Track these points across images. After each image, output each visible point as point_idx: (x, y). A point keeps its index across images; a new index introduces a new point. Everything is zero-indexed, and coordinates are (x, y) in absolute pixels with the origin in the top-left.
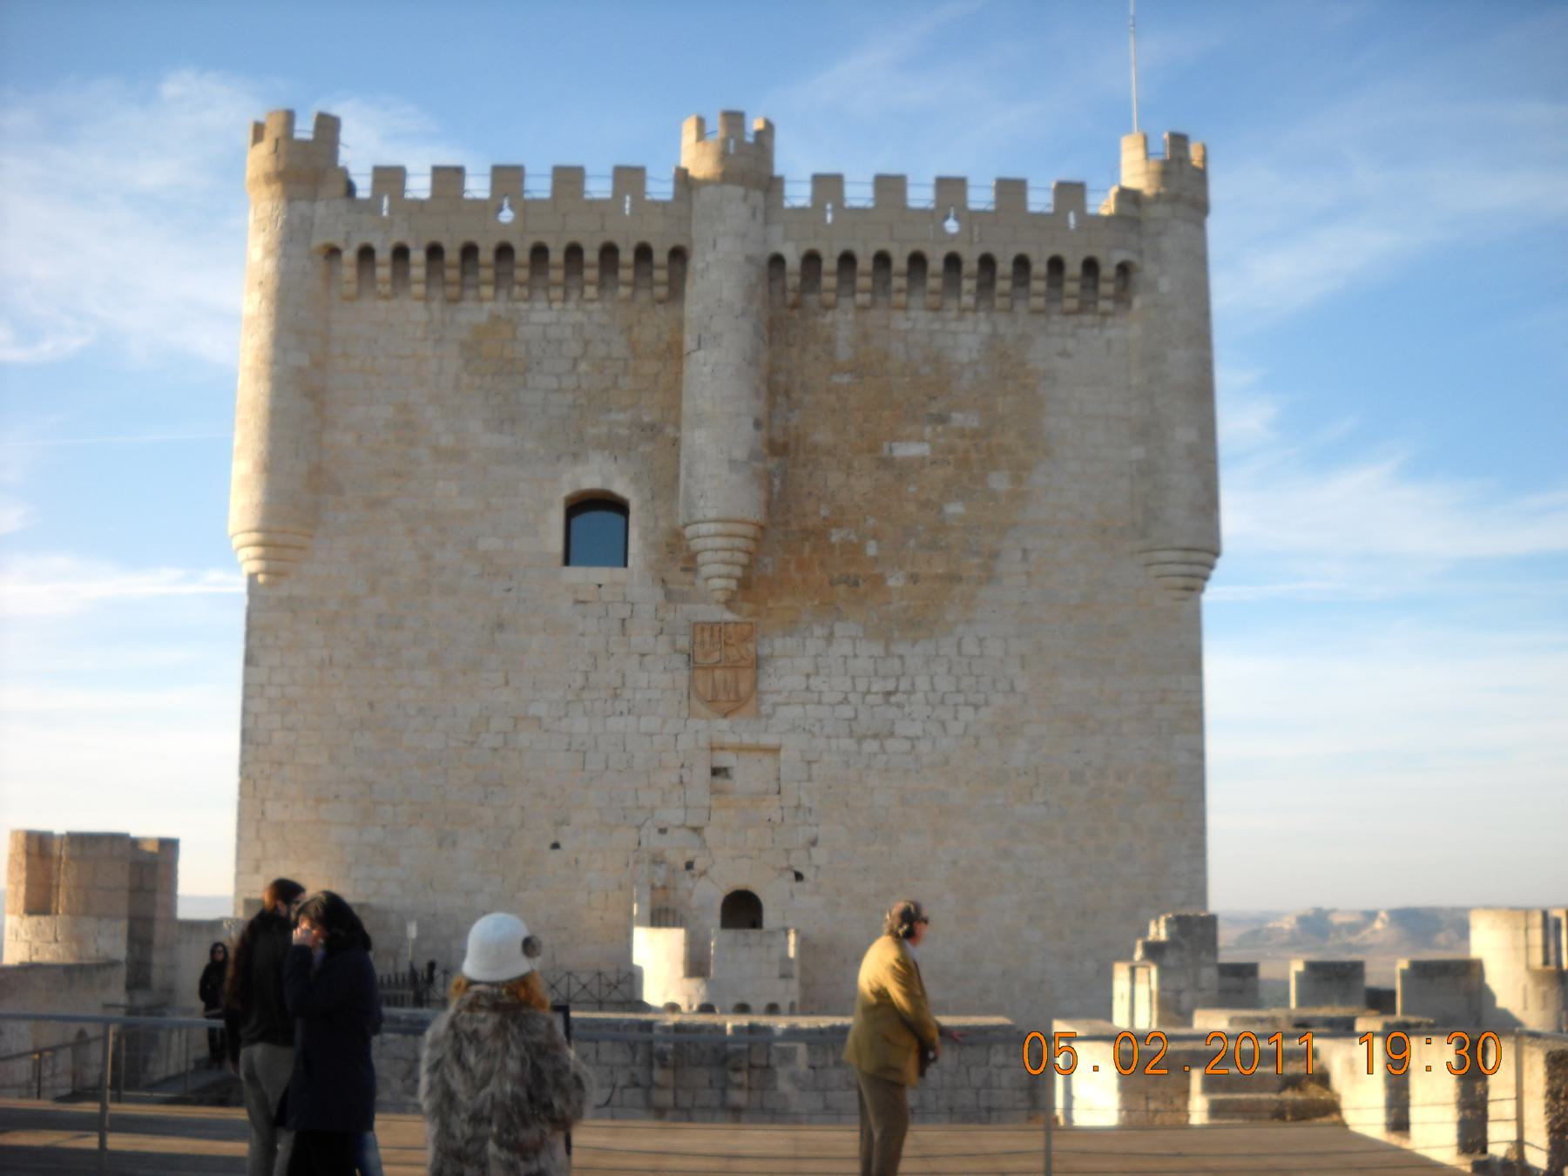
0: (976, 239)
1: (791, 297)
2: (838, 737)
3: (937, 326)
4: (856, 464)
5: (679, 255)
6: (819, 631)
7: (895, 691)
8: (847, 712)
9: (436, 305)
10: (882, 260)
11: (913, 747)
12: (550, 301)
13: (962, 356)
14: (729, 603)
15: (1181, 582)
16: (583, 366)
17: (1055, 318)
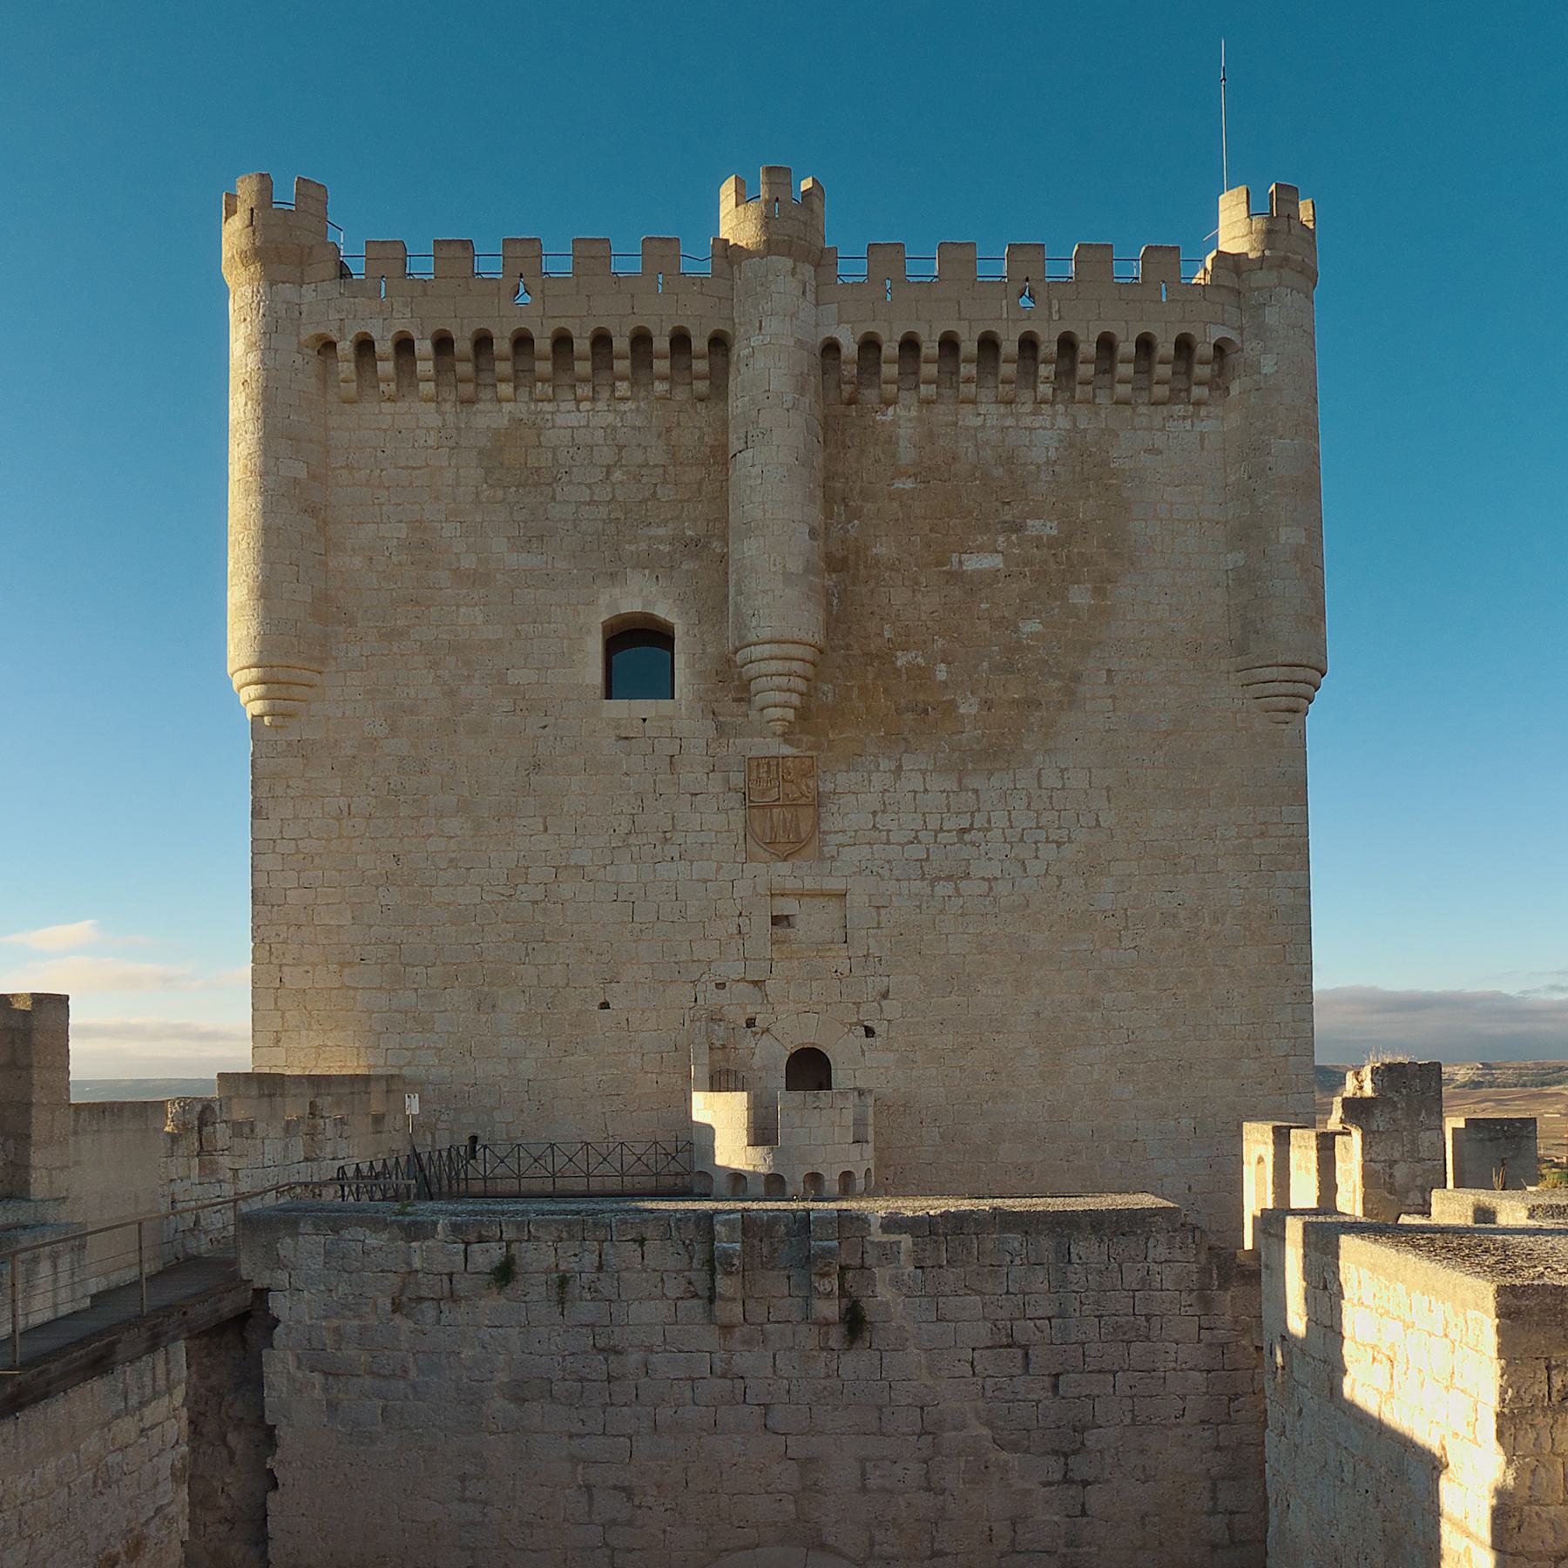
1: (847, 389)
2: (909, 879)
3: (1010, 422)
4: (923, 579)
5: (720, 343)
6: (884, 764)
7: (971, 828)
9: (447, 407)
10: (949, 344)
12: (578, 401)
13: (1038, 455)
14: (786, 737)
16: (618, 475)
17: (1142, 409)
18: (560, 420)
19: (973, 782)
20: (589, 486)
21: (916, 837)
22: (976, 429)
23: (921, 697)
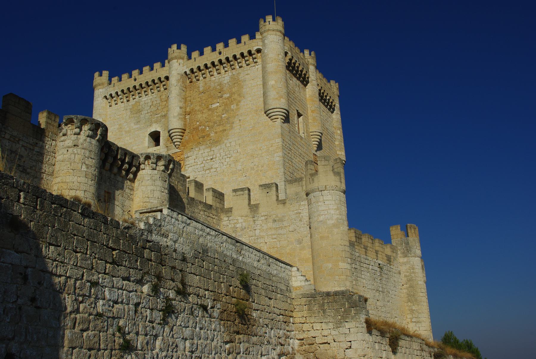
3: (220, 77)
4: (204, 112)
5: (167, 78)
6: (196, 149)
8: (203, 165)
11: (216, 170)
13: (225, 82)
16: (152, 107)
18: (143, 100)
19: (212, 149)
20: (147, 110)
22: (214, 80)
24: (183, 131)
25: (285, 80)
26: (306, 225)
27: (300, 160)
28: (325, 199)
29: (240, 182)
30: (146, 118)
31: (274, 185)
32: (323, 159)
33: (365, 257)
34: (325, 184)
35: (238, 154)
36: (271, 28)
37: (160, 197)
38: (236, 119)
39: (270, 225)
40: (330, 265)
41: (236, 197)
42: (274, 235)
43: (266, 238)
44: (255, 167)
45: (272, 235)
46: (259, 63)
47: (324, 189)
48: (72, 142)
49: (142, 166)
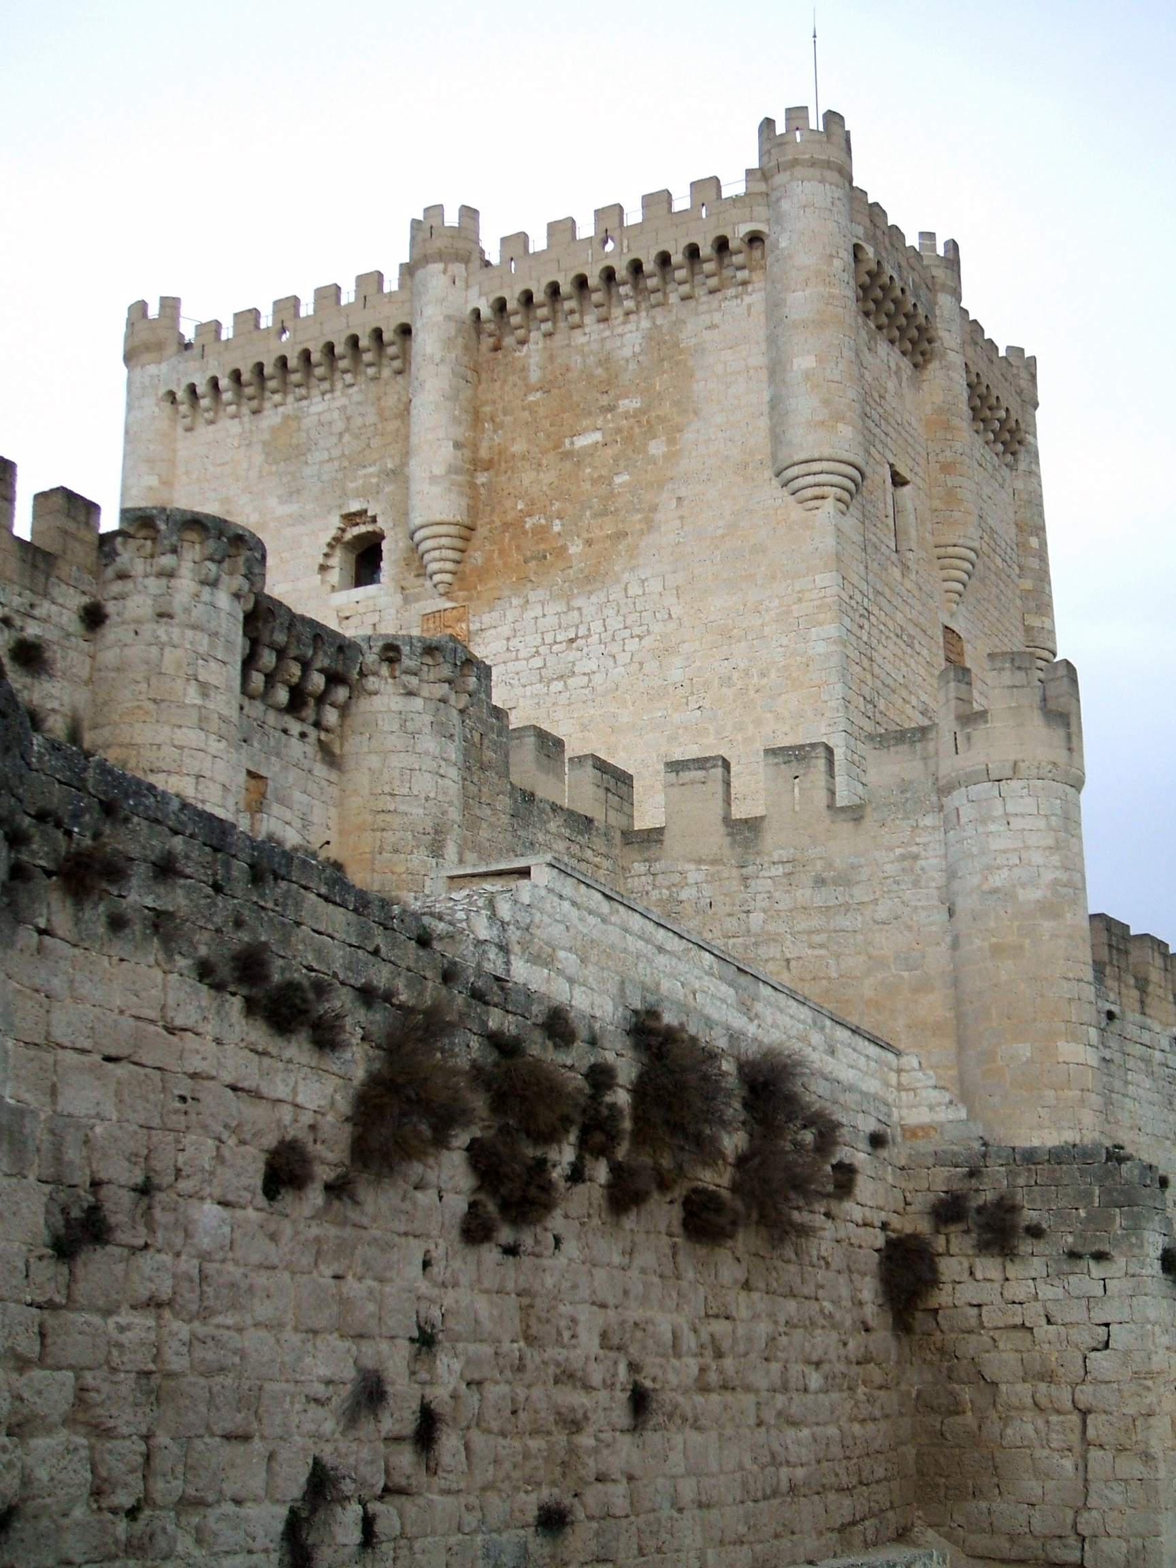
0: (625, 250)
2: (531, 684)
3: (607, 333)
4: (544, 462)
5: (405, 331)
6: (515, 601)
7: (577, 637)
8: (537, 662)
9: (246, 419)
11: (590, 681)
13: (627, 352)
15: (809, 493)
16: (347, 438)
17: (704, 299)
18: (314, 409)
19: (576, 603)
21: (537, 652)
22: (583, 345)
23: (542, 546)
24: (465, 533)
25: (852, 354)
26: (936, 903)
27: (900, 653)
28: (1010, 809)
29: (681, 731)
30: (325, 477)
31: (821, 752)
32: (1008, 665)
33: (1138, 1017)
34: (1012, 757)
35: (672, 625)
36: (807, 156)
37: (432, 795)
38: (665, 495)
39: (804, 894)
40: (1025, 1050)
41: (676, 790)
42: (818, 932)
43: (788, 943)
44: (735, 675)
45: (810, 932)
46: (757, 286)
47: (1009, 773)
48: (150, 602)
49: (372, 683)
